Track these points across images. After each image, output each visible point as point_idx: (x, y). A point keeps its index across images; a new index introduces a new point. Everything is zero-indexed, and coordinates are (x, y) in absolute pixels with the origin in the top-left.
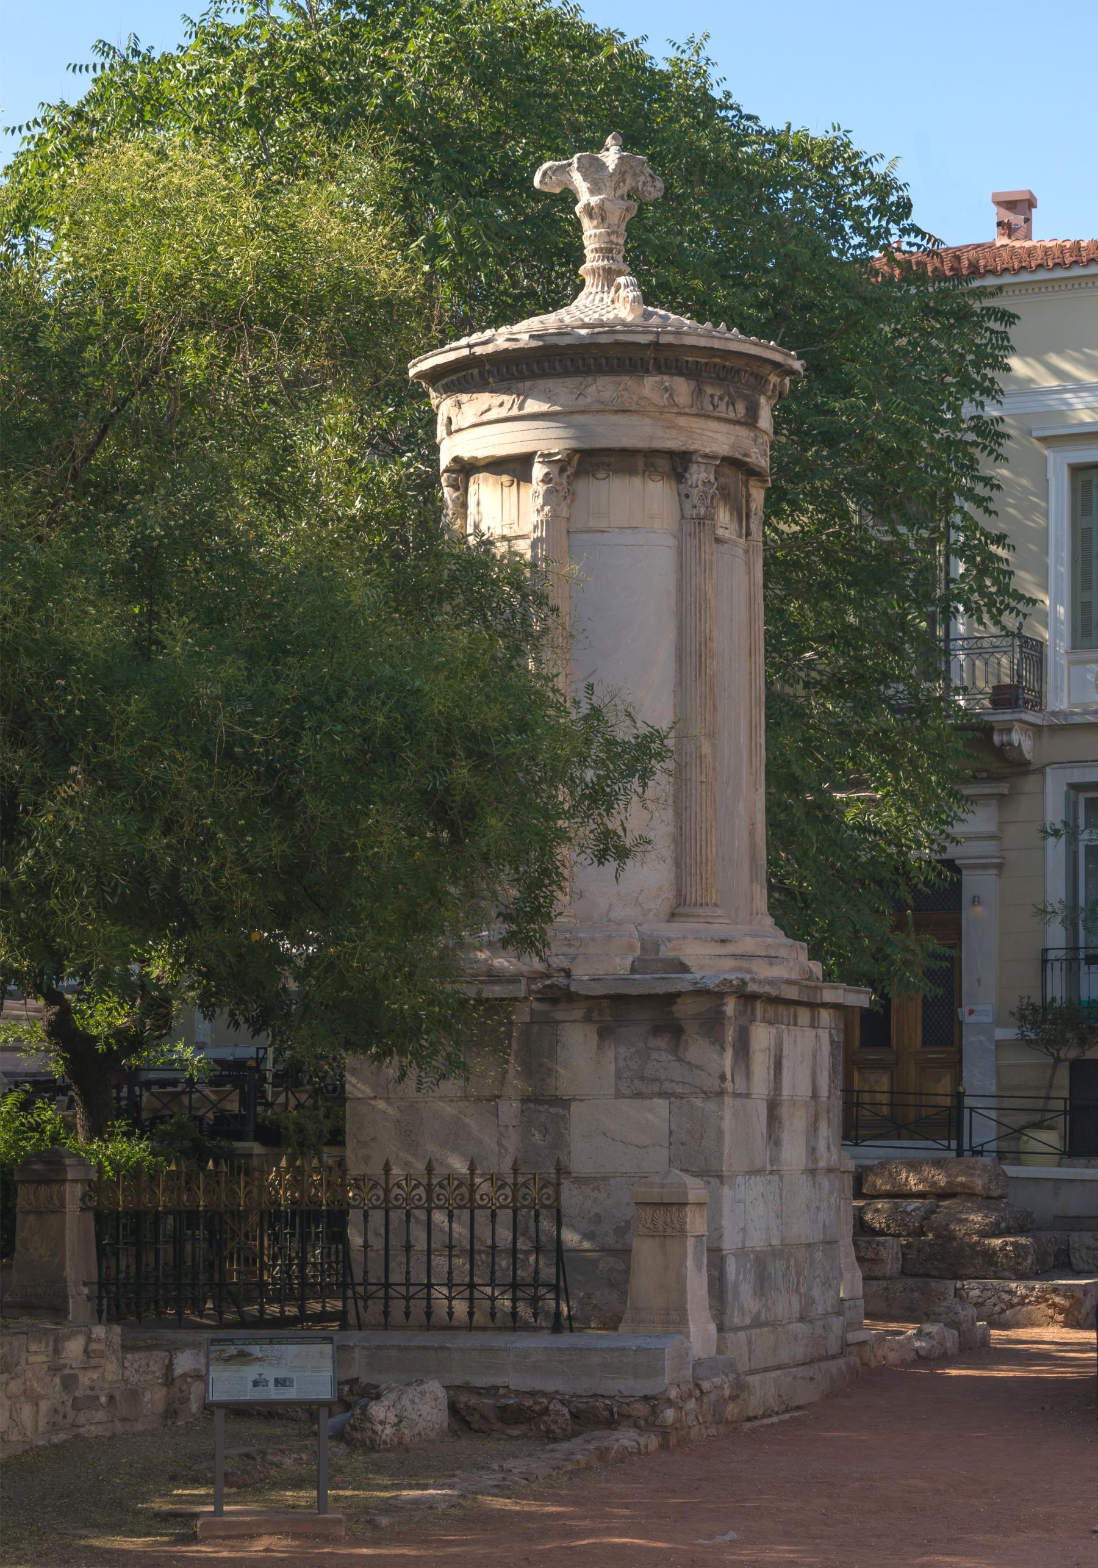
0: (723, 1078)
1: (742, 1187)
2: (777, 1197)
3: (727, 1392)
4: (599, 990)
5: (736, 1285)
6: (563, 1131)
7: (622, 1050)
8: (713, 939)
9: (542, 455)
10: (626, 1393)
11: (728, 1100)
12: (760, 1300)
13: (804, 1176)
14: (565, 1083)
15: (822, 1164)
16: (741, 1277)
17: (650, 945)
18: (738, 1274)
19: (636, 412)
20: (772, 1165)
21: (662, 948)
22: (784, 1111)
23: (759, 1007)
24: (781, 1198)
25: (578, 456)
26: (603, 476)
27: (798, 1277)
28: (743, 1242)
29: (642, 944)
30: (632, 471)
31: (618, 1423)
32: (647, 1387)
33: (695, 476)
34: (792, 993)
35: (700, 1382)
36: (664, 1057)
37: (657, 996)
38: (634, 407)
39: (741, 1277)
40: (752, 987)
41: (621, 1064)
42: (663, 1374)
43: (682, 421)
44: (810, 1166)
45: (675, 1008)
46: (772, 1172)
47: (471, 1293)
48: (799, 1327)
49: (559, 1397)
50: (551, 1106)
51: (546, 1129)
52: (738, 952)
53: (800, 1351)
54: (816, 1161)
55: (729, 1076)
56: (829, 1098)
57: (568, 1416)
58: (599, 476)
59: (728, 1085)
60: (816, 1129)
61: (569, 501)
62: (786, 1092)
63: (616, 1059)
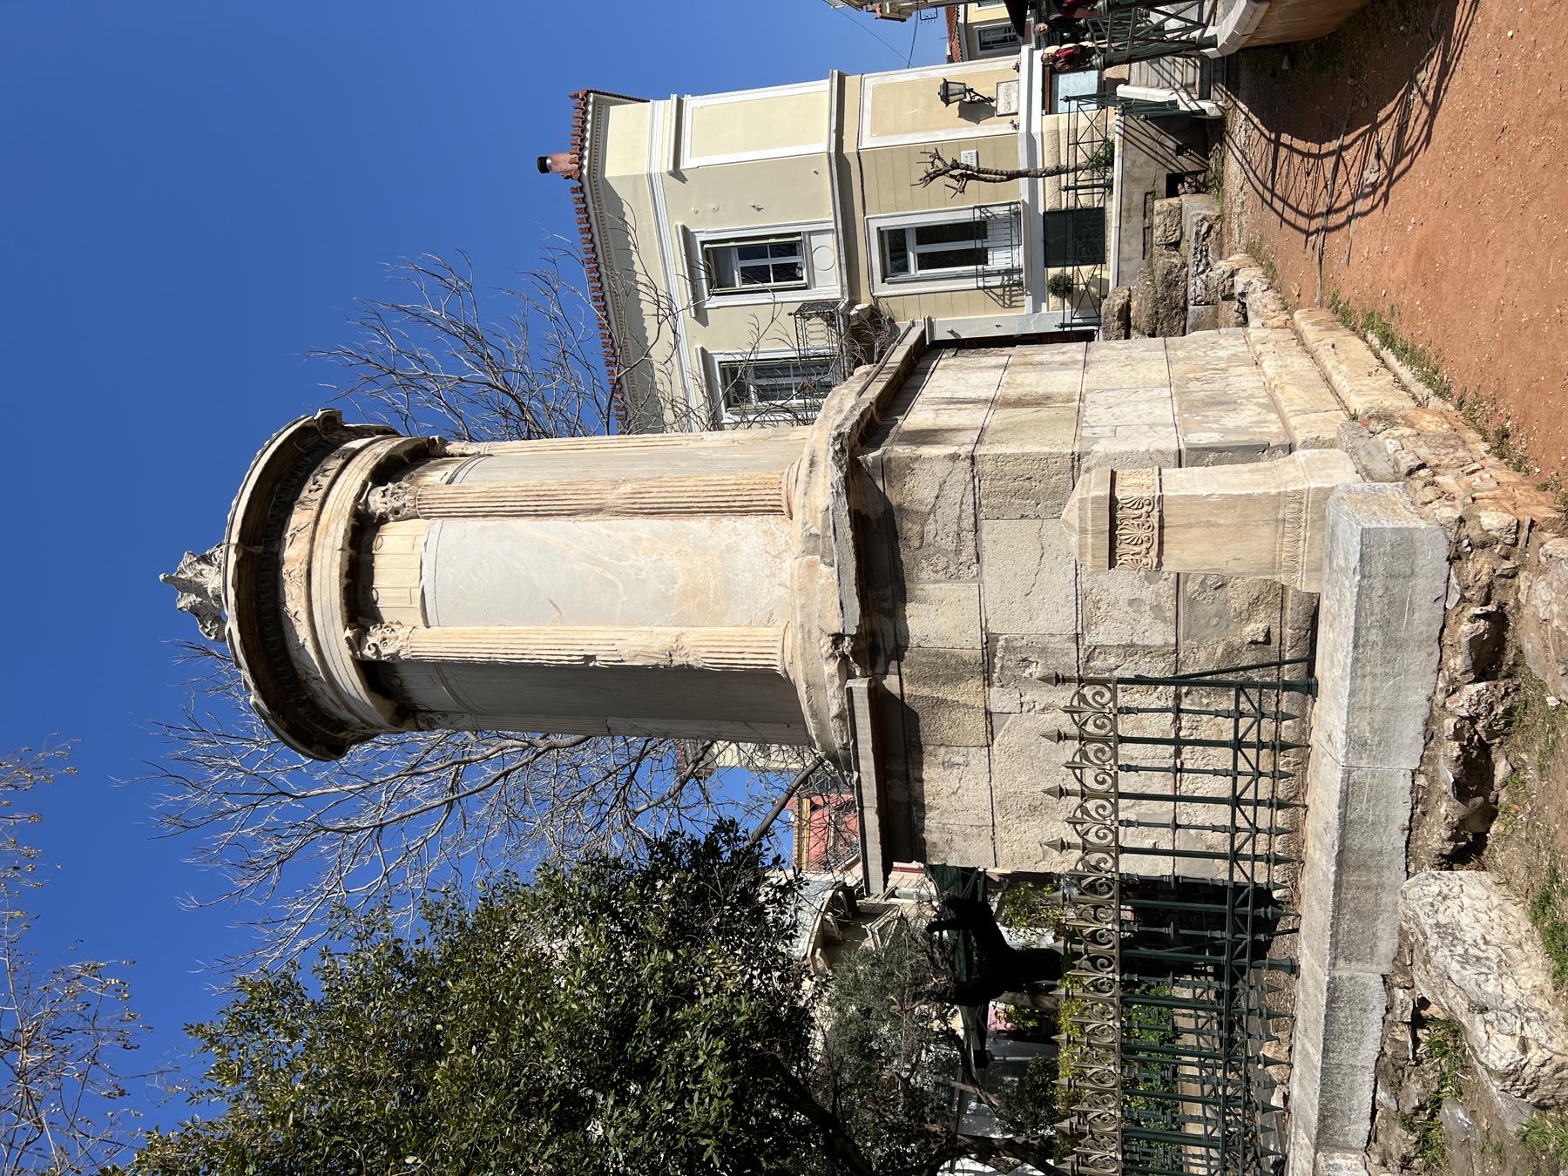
0: (954, 457)
1: (1096, 430)
2: (1110, 394)
3: (1407, 431)
4: (854, 607)
5: (1225, 431)
6: (1024, 642)
7: (924, 575)
9: (354, 653)
10: (1441, 592)
11: (981, 450)
12: (1241, 404)
13: (1091, 371)
14: (968, 644)
15: (1080, 357)
16: (1215, 426)
17: (812, 541)
18: (1213, 430)
19: (310, 563)
20: (1074, 401)
22: (1013, 393)
24: (1114, 390)
25: (360, 619)
26: (374, 593)
27: (1207, 370)
28: (1166, 425)
29: (808, 554)
31: (1501, 606)
32: (1433, 557)
33: (379, 505)
35: (1404, 469)
36: (930, 528)
37: (855, 538)
38: (304, 567)
39: (1215, 426)
40: (846, 429)
41: (941, 575)
42: (1411, 531)
45: (873, 516)
47: (1248, 803)
48: (1269, 365)
49: (1440, 697)
50: (995, 656)
51: (1024, 660)
53: (1300, 363)
54: (1075, 362)
55: (950, 450)
57: (1482, 685)
58: (375, 597)
59: (964, 451)
60: (1041, 364)
61: (394, 627)
62: (990, 393)
63: (936, 582)
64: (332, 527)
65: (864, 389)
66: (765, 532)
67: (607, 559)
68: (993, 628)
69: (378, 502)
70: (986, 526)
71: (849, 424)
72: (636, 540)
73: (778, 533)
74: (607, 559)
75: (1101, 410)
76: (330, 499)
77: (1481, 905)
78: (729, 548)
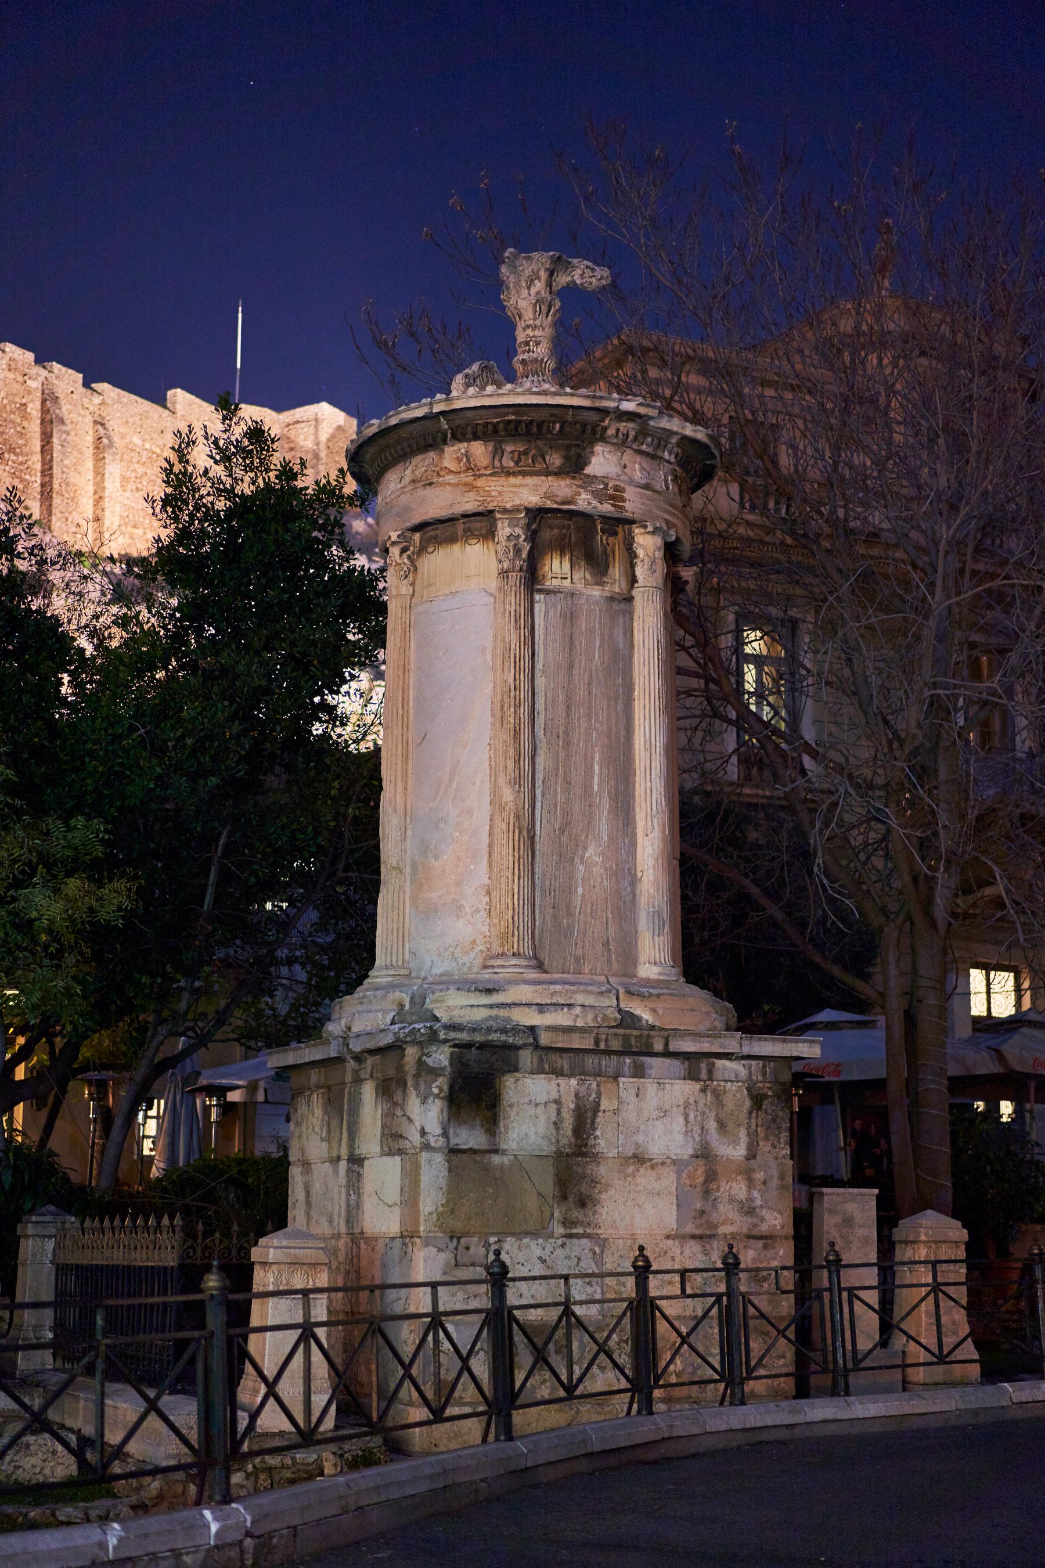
0: (423, 1133)
8: (477, 990)
21: (428, 1000)
23: (526, 1058)
25: (417, 536)
30: (452, 540)
34: (588, 1044)
43: (481, 482)
44: (690, 1228)
46: (570, 1236)
52: (509, 1001)
56: (751, 1156)
58: (430, 550)
64: (472, 495)
65: (567, 1030)
66: (474, 942)
67: (454, 786)
68: (366, 1162)
69: (504, 530)
70: (398, 1159)
71: (453, 1035)
72: (470, 812)
73: (473, 954)
74: (454, 786)
75: (538, 1252)
76: (502, 480)
77: (47, 1471)
78: (460, 908)
